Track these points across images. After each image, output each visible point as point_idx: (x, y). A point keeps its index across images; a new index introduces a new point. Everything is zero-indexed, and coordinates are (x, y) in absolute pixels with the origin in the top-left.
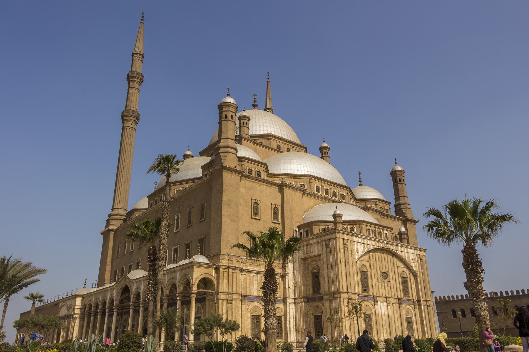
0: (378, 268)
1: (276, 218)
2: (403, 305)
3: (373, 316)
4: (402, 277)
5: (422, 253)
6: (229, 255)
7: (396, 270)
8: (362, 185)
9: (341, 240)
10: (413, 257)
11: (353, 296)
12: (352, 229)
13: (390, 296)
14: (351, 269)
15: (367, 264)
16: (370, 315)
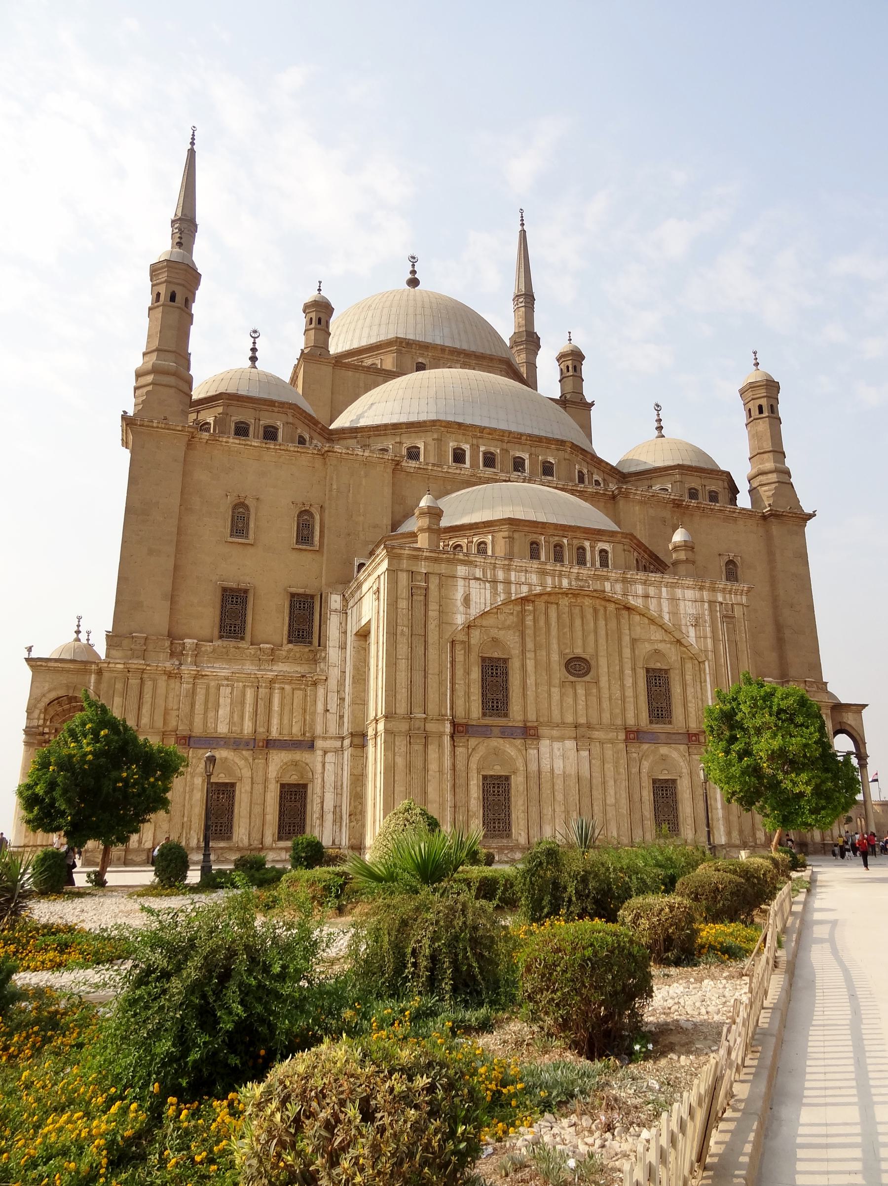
0: (555, 646)
1: (304, 536)
2: (645, 746)
3: (517, 782)
4: (648, 670)
5: (734, 599)
6: (133, 637)
7: (627, 652)
8: (663, 436)
9: (403, 578)
10: (691, 611)
11: (431, 727)
12: (482, 548)
13: (594, 721)
14: (433, 653)
15: (511, 640)
16: (507, 778)
